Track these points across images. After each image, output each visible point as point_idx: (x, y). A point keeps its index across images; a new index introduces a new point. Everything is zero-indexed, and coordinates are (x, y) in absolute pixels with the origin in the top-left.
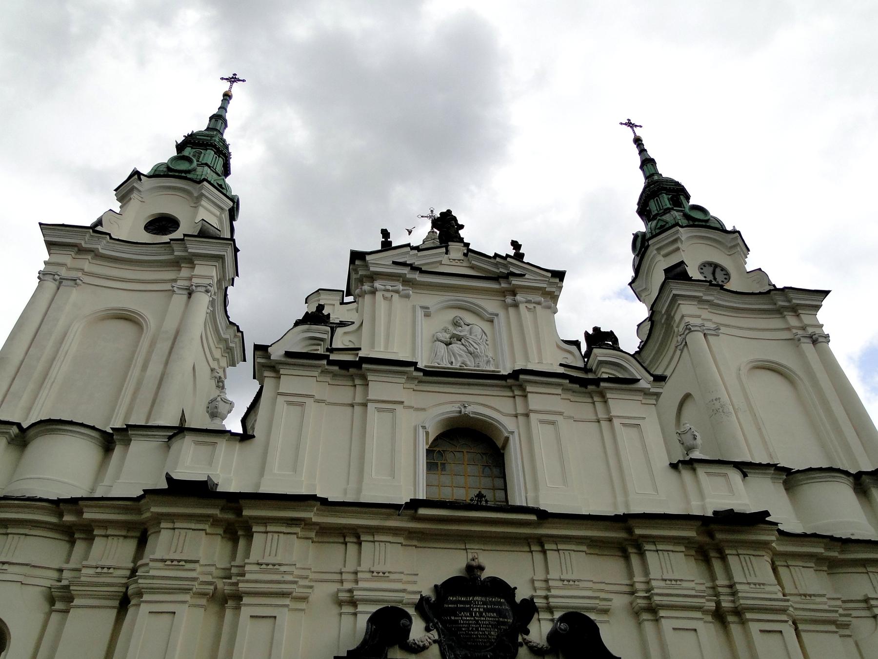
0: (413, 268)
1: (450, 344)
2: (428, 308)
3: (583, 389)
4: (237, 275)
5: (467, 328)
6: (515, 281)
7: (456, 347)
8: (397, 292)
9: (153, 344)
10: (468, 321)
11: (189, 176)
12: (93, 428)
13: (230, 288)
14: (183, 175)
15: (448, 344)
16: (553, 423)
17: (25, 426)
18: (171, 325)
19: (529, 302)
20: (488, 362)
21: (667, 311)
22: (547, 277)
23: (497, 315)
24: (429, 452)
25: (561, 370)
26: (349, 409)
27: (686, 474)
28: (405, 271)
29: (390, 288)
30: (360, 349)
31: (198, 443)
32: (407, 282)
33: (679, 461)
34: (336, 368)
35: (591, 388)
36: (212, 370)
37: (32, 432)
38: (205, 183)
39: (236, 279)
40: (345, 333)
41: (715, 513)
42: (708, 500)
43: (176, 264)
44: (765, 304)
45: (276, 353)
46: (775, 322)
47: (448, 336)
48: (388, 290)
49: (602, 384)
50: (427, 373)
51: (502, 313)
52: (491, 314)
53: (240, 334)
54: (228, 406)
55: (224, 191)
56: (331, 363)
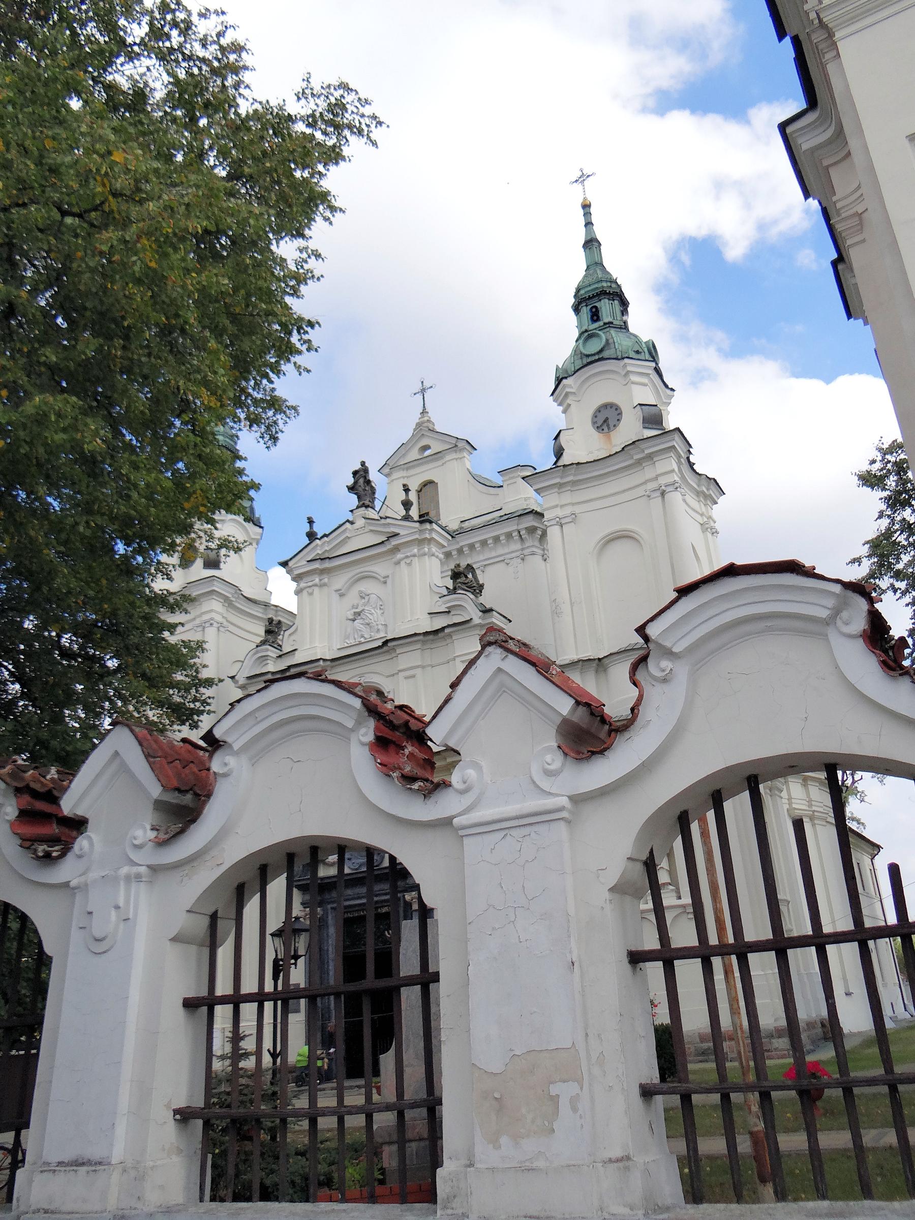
5: (367, 598)
6: (394, 542)
8: (316, 585)
15: (354, 620)
19: (407, 557)
28: (317, 565)
29: (310, 584)
32: (322, 572)
35: (441, 635)
44: (625, 461)
46: (636, 478)
48: (310, 587)
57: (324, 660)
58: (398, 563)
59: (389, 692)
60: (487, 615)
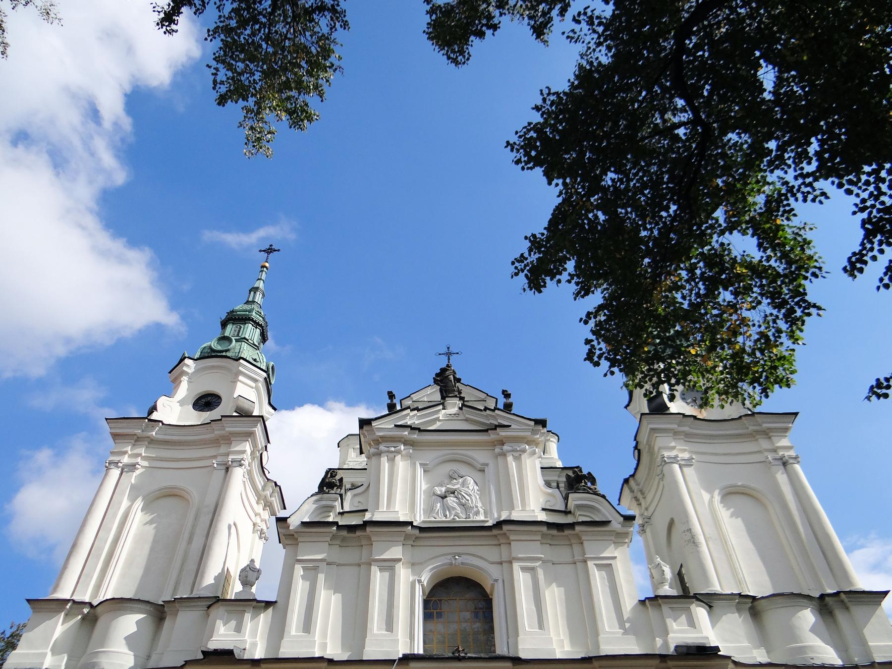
0: (412, 428)
1: (446, 497)
2: (427, 465)
3: (560, 534)
4: (269, 442)
6: (503, 433)
7: (451, 500)
9: (196, 517)
10: (463, 473)
11: (228, 354)
12: (148, 602)
13: (265, 453)
14: (224, 354)
16: (532, 569)
17: (95, 604)
18: (210, 500)
19: (516, 451)
20: (477, 513)
21: (648, 441)
22: (529, 426)
23: (487, 465)
24: (426, 603)
25: (542, 517)
26: (356, 568)
27: (652, 612)
29: (393, 449)
30: (366, 510)
31: (228, 612)
33: (647, 598)
34: (344, 533)
35: (567, 532)
36: (254, 525)
37: (99, 609)
38: (241, 361)
39: (268, 445)
40: (355, 495)
41: (677, 647)
42: (671, 635)
43: (216, 442)
44: (737, 429)
45: (294, 523)
46: (750, 446)
47: (443, 489)
49: (578, 528)
50: (422, 529)
51: (491, 463)
52: (482, 465)
53: (278, 489)
54: (256, 574)
55: (258, 364)
56: (340, 527)
57: (413, 526)
58: (504, 455)
59: (496, 580)
60: (627, 523)
